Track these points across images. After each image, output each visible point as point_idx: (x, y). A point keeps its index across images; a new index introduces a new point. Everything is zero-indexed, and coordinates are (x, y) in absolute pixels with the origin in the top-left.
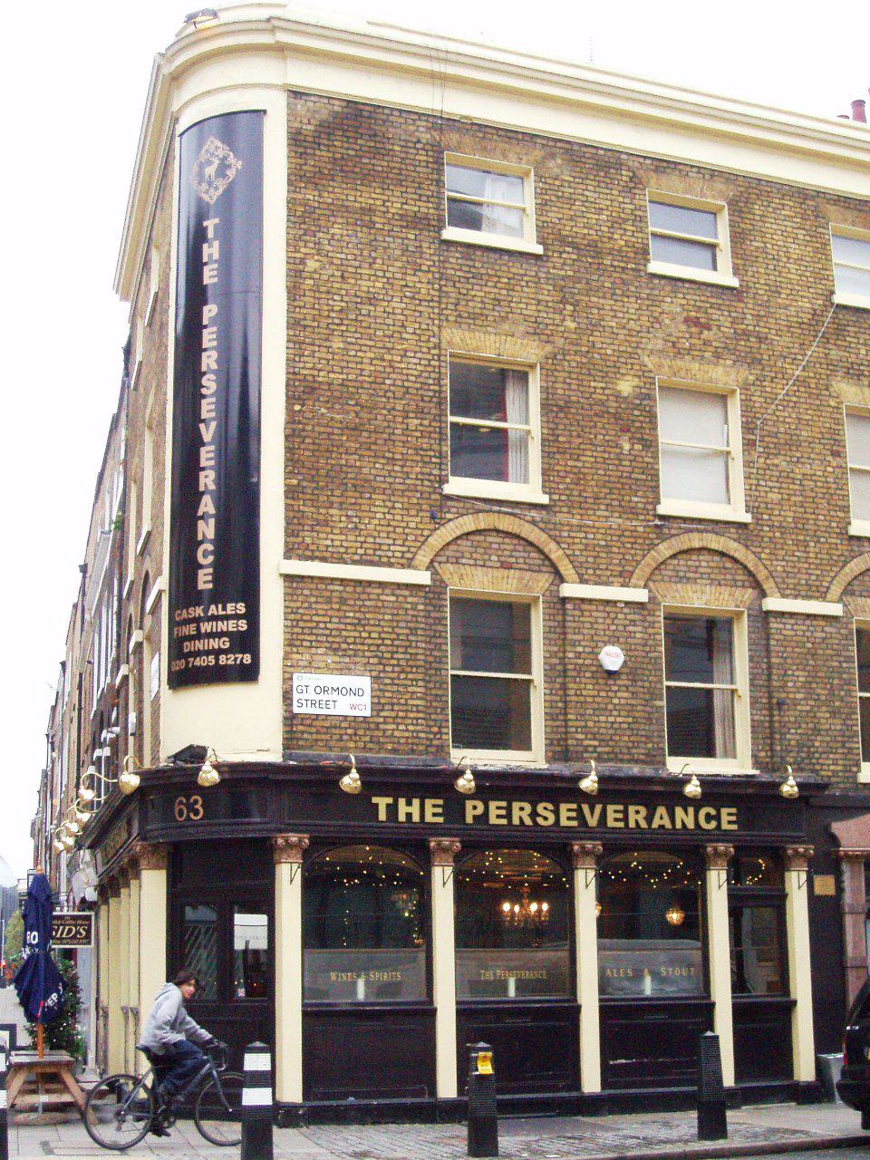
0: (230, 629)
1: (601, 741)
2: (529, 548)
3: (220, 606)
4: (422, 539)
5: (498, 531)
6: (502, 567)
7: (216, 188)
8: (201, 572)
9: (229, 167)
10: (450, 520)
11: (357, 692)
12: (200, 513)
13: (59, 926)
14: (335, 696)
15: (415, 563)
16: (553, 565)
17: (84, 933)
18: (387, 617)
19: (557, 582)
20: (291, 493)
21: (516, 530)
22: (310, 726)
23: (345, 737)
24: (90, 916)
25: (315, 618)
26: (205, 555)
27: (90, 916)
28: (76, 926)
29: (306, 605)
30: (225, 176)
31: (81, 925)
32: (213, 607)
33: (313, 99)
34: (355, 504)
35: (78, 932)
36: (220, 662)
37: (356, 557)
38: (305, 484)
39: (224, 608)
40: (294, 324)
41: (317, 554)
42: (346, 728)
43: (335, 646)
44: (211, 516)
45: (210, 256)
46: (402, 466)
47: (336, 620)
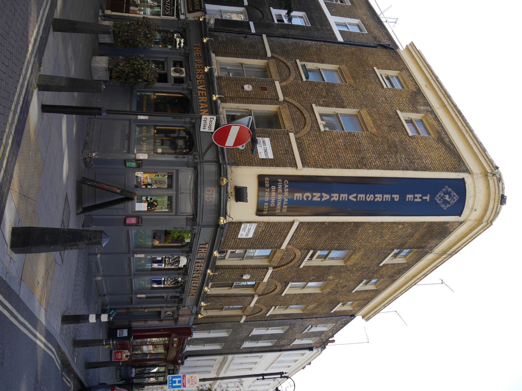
0: (277, 207)
1: (220, 274)
2: (286, 263)
3: (287, 203)
4: (296, 247)
5: (294, 258)
6: (282, 258)
7: (440, 200)
9: (446, 205)
10: (301, 251)
11: (247, 235)
12: (323, 194)
13: (170, 4)
14: (246, 231)
15: (289, 245)
16: (279, 267)
17: (167, 13)
18: (272, 241)
19: (273, 267)
20: (323, 223)
21: (294, 261)
22: (237, 227)
23: (231, 233)
24: (174, 16)
25: (276, 228)
26: (307, 197)
27: (174, 16)
28: (170, 10)
29: (281, 226)
30: (443, 203)
31: (170, 12)
33: (457, 226)
34: (313, 235)
35: (167, 11)
36: (265, 203)
37: (294, 235)
38: (325, 226)
39: (285, 205)
40: (382, 223)
41: (299, 228)
42: (234, 233)
43: (265, 231)
44: (321, 199)
45: (416, 198)
46: (322, 243)
47: (274, 231)
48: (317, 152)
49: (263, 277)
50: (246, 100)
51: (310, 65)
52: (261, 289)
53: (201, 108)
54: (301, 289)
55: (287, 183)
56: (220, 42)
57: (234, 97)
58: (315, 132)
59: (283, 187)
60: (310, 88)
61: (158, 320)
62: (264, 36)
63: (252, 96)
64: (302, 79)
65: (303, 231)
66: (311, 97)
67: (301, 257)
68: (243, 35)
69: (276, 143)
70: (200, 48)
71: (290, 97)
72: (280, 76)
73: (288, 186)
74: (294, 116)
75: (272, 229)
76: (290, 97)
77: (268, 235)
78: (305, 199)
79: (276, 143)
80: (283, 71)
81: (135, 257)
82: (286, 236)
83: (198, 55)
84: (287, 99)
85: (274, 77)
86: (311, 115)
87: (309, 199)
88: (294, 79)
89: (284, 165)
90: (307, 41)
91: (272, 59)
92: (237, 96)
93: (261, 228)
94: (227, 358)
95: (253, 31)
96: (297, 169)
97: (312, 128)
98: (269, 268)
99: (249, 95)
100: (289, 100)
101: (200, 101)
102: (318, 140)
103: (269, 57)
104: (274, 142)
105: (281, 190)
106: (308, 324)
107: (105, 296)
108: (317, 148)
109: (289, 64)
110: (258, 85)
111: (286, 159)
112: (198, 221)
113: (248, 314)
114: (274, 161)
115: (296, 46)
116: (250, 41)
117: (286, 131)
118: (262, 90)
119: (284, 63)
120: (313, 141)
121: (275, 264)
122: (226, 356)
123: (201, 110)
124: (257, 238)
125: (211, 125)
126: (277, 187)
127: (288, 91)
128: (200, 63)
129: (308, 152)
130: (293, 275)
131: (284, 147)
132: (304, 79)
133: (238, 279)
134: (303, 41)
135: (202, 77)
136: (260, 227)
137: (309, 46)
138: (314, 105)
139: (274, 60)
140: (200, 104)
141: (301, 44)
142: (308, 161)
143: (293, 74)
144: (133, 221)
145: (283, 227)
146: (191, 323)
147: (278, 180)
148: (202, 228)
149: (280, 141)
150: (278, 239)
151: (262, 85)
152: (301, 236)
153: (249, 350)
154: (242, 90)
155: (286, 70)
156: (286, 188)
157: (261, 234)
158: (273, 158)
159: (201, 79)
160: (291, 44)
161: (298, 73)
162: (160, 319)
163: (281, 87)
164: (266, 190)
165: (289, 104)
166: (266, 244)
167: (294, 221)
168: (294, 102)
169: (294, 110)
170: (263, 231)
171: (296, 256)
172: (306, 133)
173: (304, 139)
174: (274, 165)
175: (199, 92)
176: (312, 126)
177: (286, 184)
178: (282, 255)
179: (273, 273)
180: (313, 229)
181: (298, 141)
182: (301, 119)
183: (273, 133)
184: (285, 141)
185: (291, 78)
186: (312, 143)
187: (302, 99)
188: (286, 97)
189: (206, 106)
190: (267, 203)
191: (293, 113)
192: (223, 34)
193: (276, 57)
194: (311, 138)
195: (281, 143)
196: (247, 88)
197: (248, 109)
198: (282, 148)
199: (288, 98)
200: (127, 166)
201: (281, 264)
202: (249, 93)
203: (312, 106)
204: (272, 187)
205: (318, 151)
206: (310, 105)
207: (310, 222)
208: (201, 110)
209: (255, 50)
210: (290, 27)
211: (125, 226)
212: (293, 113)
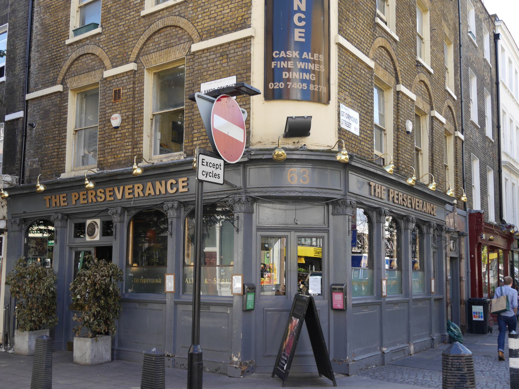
2: (391, 63)
3: (310, 54)
6: (385, 69)
8: (297, 31)
10: (377, 37)
16: (396, 74)
22: (344, 136)
23: (353, 146)
25: (346, 74)
26: (300, 19)
32: (305, 53)
36: (310, 88)
39: (313, 56)
41: (346, 37)
42: (353, 140)
47: (350, 77)
48: (224, 5)
49: (409, 100)
50: (137, 122)
51: (75, 22)
52: (423, 106)
53: (153, 194)
54: (423, 43)
55: (278, 52)
56: (41, 165)
57: (132, 142)
58: (189, 9)
59: (285, 59)
60: (114, 20)
61: (460, 261)
62: (28, 97)
63: (131, 113)
64: (99, 34)
65: (350, 31)
66: (128, 18)
67: (385, 38)
68: (28, 131)
69: (209, 73)
70: (53, 197)
71: (129, 53)
72: (95, 70)
73: (283, 52)
74: (161, 45)
75: (348, 81)
76: (129, 53)
77: (355, 87)
78: (303, 23)
79: (209, 73)
80: (85, 66)
81: (385, 295)
82: (357, 58)
83: (65, 199)
84: (133, 57)
85: (97, 80)
86: (159, 16)
87: (303, 16)
88: (99, 46)
89: (248, 58)
90: (34, 29)
91: (66, 84)
92: (131, 137)
93: (346, 97)
94: (506, 162)
95: (20, 114)
96: (253, 37)
97: (182, 15)
98: (397, 90)
99: (128, 118)
100: (136, 54)
101: (141, 194)
102: (202, 4)
103: (64, 88)
104: (208, 76)
105: (289, 62)
106: (467, 38)
107: (433, 339)
108: (217, 5)
109: (74, 56)
110: (111, 104)
111: (238, 55)
112: (339, 197)
113: (453, 128)
114: (240, 74)
115: (43, 47)
116: (37, 119)
117: (189, 57)
118: (119, 98)
119: (72, 64)
120: (205, 13)
121: (393, 80)
122: (502, 164)
123: (158, 193)
124: (359, 105)
125: (214, 165)
126: (284, 69)
127: (119, 56)
128: (77, 196)
129: (223, 20)
130: (407, 54)
131: (215, 60)
132: (99, 30)
133: (412, 139)
134: (34, 34)
135: (100, 192)
136: (345, 99)
137: (42, 24)
138: (143, 13)
139: (68, 81)
140: (147, 194)
141: (38, 37)
142: (240, 18)
143: (91, 48)
144: (338, 298)
145: (345, 63)
146: (464, 213)
147: (273, 67)
148: (350, 191)
149: (205, 66)
150: (360, 71)
151: (111, 98)
152: (357, 35)
153: (496, 129)
154: (120, 129)
155: (83, 60)
156: (286, 54)
157: (354, 98)
158: (235, 77)
159: (104, 193)
160: (40, 53)
161: (88, 41)
162: (458, 259)
163: (113, 67)
164: (289, 87)
165: (141, 54)
166: (367, 92)
167: (337, 44)
168: (138, 46)
169: (151, 45)
170: (351, 94)
171: (384, 45)
172: (191, 25)
173: (201, 27)
174: (248, 74)
175: (127, 196)
176: (178, 15)
177: (279, 54)
178: (380, 68)
179: (404, 84)
180: (348, 13)
181: (204, 36)
182: (166, 33)
183: (191, 78)
184: (205, 59)
185: (98, 51)
186: (208, 13)
187: (133, 32)
188: (130, 59)
189: (149, 185)
190: (311, 85)
191: (157, 46)
192: (28, 162)
193: (62, 77)
194: (200, 16)
195: (209, 65)
196: (116, 120)
197: (152, 119)
198: (218, 63)
199: (132, 56)
200: (252, 308)
201: (392, 70)
202: (125, 118)
203: (144, 17)
204: (284, 77)
205: (222, 4)
206: (142, 20)
207: (338, 17)
208: (158, 193)
209: (51, 110)
210: (12, 56)
211: (346, 309)
212: (157, 46)
